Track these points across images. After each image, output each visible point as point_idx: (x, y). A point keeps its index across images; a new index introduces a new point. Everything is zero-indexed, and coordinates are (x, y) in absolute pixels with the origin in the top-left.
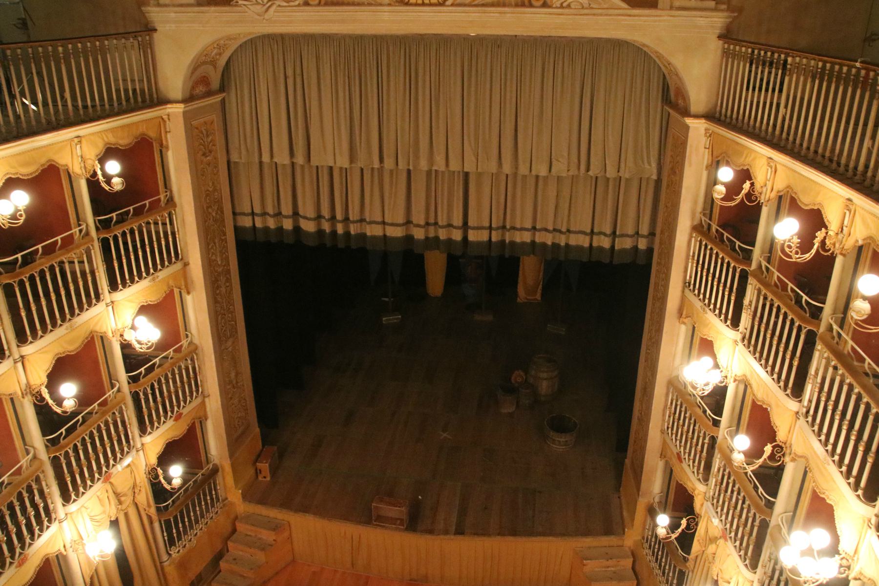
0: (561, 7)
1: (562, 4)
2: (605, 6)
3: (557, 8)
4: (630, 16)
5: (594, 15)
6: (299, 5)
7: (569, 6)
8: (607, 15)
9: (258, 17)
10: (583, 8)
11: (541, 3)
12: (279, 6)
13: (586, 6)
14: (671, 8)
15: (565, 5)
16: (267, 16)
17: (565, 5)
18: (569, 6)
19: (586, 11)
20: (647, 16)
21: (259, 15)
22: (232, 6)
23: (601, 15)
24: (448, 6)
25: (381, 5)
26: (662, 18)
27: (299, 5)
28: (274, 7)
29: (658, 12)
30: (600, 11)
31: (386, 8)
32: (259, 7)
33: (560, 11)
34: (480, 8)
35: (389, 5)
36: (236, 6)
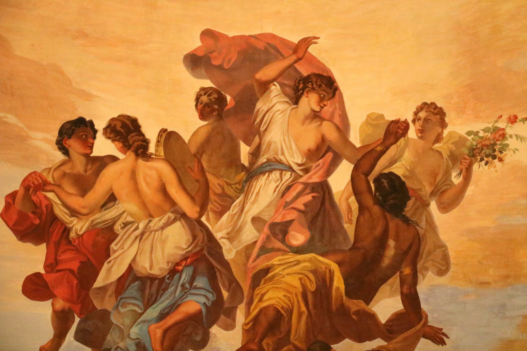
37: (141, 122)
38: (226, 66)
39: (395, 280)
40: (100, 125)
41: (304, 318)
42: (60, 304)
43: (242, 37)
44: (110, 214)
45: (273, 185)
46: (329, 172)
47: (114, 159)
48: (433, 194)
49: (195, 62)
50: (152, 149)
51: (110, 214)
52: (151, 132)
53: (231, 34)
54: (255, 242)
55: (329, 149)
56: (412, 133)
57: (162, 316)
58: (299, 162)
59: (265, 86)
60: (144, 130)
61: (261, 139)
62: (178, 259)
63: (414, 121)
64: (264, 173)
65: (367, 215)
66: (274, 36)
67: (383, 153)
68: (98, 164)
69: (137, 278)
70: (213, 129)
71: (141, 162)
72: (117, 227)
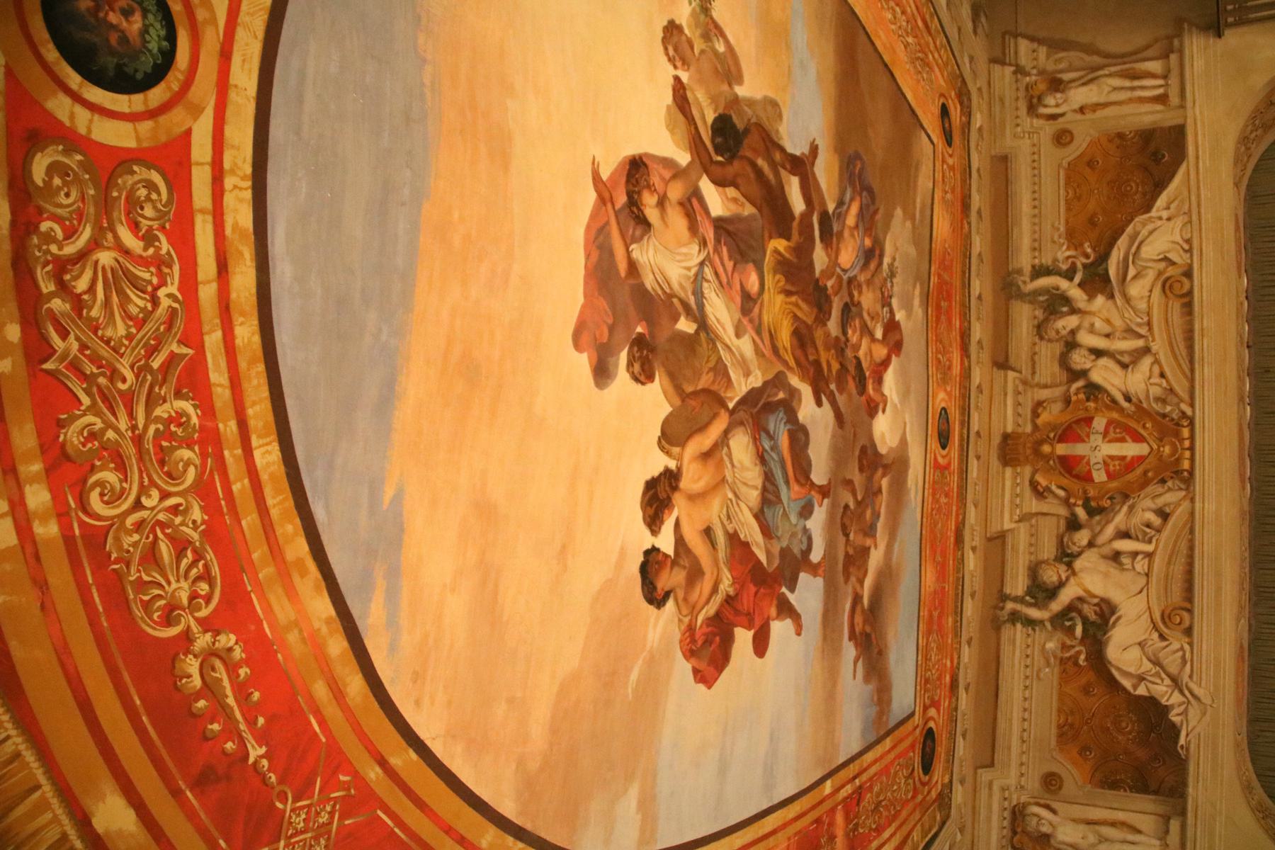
0: (1190, 251)
1: (1186, 251)
2: (1186, 193)
3: (1192, 256)
4: (1197, 158)
5: (1199, 205)
6: (1191, 644)
7: (1188, 241)
8: (1198, 188)
9: (1208, 718)
10: (1190, 222)
11: (1185, 280)
12: (1191, 677)
13: (1186, 218)
14: (1182, 107)
15: (1187, 247)
16: (1207, 701)
17: (1187, 247)
18: (1188, 241)
19: (1195, 218)
20: (1196, 135)
21: (1204, 714)
22: (1187, 756)
23: (1199, 196)
24: (1194, 412)
25: (1192, 514)
26: (1199, 117)
27: (1191, 644)
28: (1192, 685)
29: (1190, 122)
30: (1193, 198)
31: (1198, 505)
32: (1191, 712)
33: (1195, 252)
34: (1197, 366)
35: (1192, 500)
36: (1188, 750)
37: (648, 477)
38: (610, 321)
39: (783, 173)
40: (648, 541)
41: (800, 302)
42: (773, 611)
43: (586, 283)
44: (721, 539)
45: (713, 295)
46: (707, 212)
47: (677, 525)
48: (730, 85)
49: (602, 373)
50: (672, 465)
51: (721, 539)
52: (658, 463)
53: (581, 300)
54: (754, 341)
55: (689, 200)
56: (685, 77)
57: (787, 482)
58: (697, 248)
59: (633, 267)
60: (656, 474)
61: (676, 296)
62: (754, 451)
63: (675, 67)
64: (703, 305)
65: (739, 181)
66: (588, 228)
67: (696, 128)
68: (681, 550)
69: (762, 511)
70: (664, 366)
71: (683, 484)
72: (730, 529)
